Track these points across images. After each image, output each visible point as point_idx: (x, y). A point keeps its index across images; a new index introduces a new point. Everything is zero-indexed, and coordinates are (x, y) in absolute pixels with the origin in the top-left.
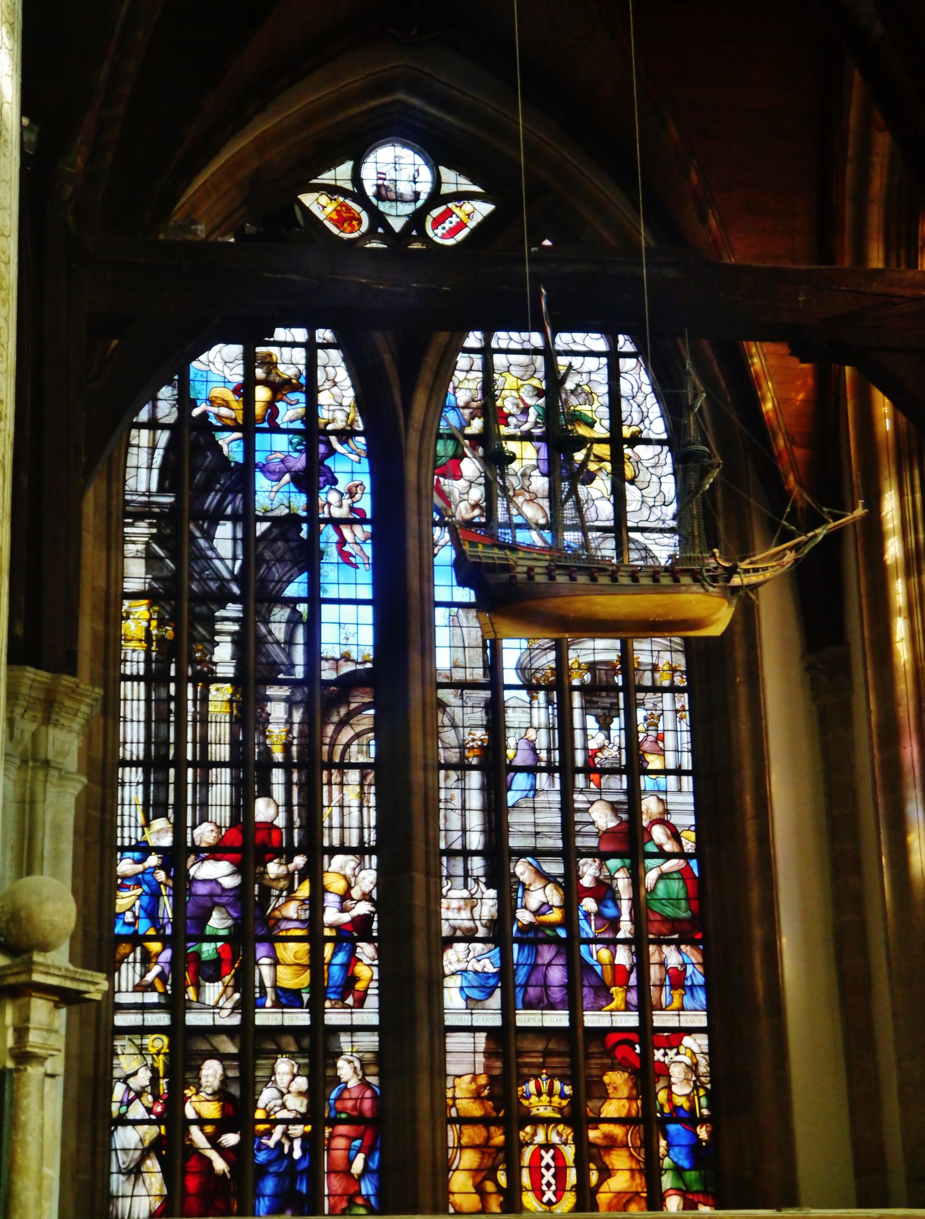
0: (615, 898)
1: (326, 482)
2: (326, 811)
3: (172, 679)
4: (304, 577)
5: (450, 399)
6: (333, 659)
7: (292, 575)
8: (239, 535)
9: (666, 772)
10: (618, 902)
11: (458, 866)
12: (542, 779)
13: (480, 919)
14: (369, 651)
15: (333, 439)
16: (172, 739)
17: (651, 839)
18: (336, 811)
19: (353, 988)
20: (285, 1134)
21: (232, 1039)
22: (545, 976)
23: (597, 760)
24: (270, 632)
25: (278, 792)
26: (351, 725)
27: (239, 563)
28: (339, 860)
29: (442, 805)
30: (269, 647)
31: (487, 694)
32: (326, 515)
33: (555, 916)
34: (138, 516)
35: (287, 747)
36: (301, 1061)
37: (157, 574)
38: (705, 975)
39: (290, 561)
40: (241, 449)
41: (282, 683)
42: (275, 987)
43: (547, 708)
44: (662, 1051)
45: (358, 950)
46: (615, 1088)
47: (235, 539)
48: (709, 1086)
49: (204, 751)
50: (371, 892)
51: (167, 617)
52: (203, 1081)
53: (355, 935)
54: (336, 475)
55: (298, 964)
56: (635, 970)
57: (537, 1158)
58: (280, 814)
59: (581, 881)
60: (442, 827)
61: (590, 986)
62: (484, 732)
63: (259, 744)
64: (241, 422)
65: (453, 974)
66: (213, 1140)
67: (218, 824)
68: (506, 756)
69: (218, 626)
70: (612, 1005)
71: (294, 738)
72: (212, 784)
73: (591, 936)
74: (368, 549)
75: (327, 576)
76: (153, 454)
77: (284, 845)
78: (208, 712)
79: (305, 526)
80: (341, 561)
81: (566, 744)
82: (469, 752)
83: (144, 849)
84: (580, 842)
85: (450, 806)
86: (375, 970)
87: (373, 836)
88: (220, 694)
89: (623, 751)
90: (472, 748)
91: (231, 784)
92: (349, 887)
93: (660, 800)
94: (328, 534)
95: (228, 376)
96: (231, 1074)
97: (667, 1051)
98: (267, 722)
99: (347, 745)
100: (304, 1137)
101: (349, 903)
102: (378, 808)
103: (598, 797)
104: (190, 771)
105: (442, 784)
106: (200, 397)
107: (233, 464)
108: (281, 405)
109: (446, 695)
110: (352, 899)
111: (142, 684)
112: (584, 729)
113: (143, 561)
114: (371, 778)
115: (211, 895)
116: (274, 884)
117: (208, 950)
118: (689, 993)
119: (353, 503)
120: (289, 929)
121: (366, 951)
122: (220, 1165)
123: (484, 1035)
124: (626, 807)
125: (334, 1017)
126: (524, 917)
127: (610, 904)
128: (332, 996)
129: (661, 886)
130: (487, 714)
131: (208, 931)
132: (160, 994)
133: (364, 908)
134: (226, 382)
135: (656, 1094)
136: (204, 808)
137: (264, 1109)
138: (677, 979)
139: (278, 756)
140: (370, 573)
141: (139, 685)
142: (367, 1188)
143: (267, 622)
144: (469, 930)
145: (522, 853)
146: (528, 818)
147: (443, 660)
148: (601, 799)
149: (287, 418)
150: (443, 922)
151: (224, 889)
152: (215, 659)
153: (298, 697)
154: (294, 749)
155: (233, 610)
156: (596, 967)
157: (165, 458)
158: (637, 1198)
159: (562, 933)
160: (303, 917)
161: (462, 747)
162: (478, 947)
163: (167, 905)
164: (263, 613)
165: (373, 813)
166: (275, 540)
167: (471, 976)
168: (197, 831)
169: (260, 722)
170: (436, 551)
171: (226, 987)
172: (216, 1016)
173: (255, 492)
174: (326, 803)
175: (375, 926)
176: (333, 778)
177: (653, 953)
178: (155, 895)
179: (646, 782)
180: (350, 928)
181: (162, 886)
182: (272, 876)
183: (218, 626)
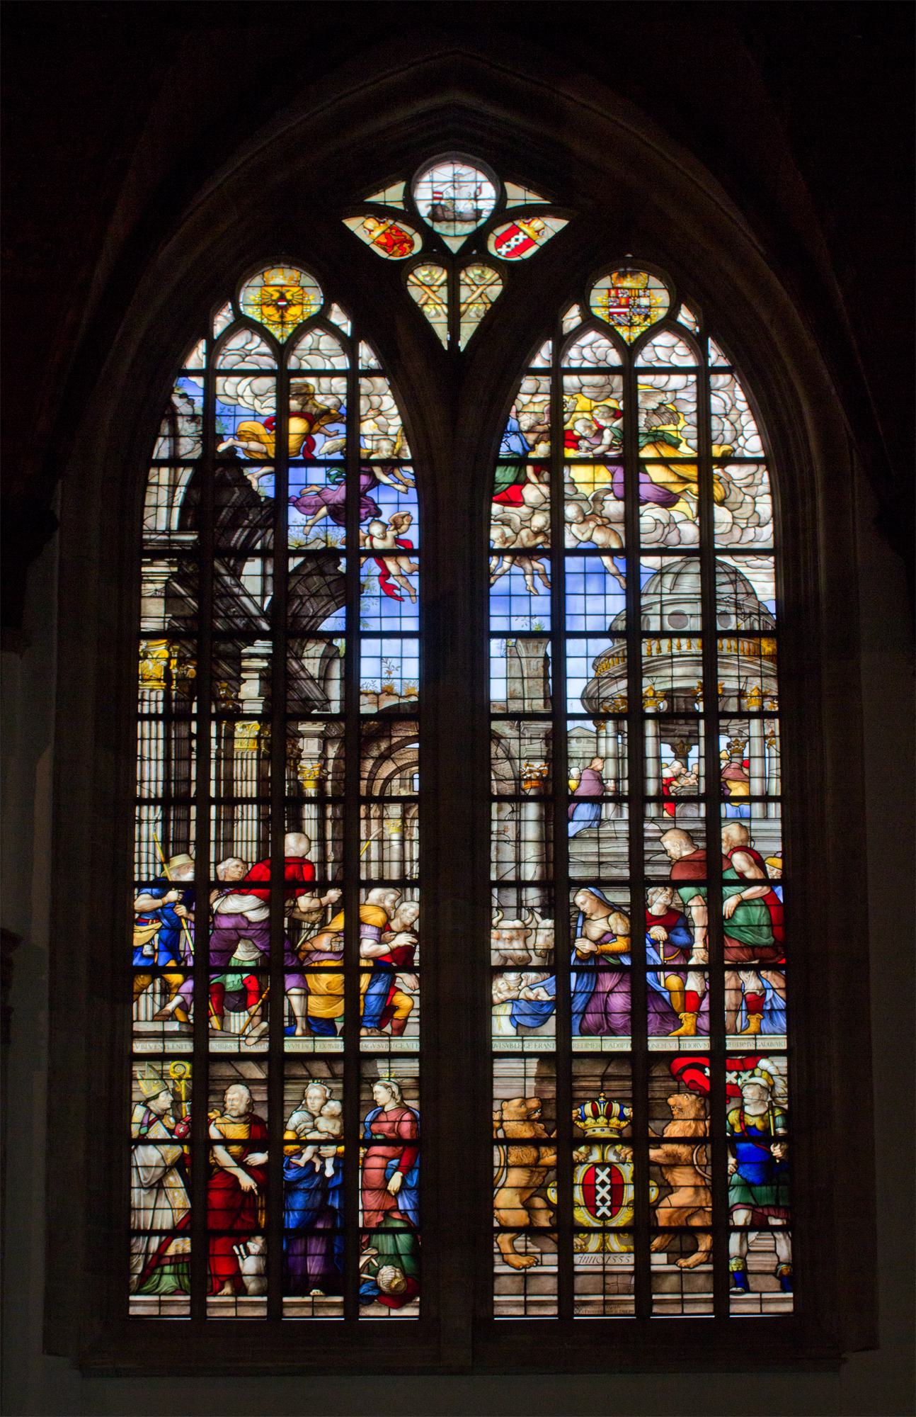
0: (688, 926)
1: (369, 514)
2: (364, 846)
3: (194, 717)
4: (342, 611)
5: (512, 424)
6: (374, 693)
7: (328, 610)
8: (270, 570)
9: (750, 799)
10: (691, 930)
11: (511, 897)
12: (609, 810)
13: (534, 949)
14: (415, 686)
15: (377, 471)
16: (194, 777)
17: (732, 867)
18: (374, 845)
19: (392, 1017)
20: (317, 1154)
21: (260, 1066)
22: (606, 1003)
23: (671, 789)
24: (303, 668)
25: (311, 827)
26: (392, 759)
27: (268, 599)
28: (376, 893)
29: (494, 837)
30: (302, 683)
31: (548, 725)
32: (368, 547)
33: (620, 944)
34: (157, 555)
35: (320, 783)
36: (333, 1086)
37: (178, 613)
38: (787, 1001)
39: (327, 596)
40: (273, 483)
41: (315, 719)
42: (306, 1017)
43: (616, 737)
44: (735, 1074)
45: (398, 980)
46: (681, 1110)
47: (264, 575)
48: (786, 1107)
49: (229, 788)
50: (412, 923)
51: (188, 655)
52: (228, 1104)
53: (394, 964)
54: (380, 506)
55: (331, 995)
56: (707, 996)
57: (591, 1176)
58: (313, 849)
59: (650, 910)
60: (493, 859)
61: (657, 1012)
62: (543, 763)
63: (289, 780)
64: (273, 456)
65: (503, 1002)
66: (241, 1163)
67: (244, 859)
68: (568, 786)
69: (245, 664)
70: (681, 1031)
71: (329, 773)
72: (238, 820)
73: (659, 963)
74: (415, 582)
75: (368, 610)
76: (174, 492)
77: (317, 879)
78: (233, 749)
79: (343, 561)
80: (383, 594)
82: (526, 783)
83: (162, 885)
84: (649, 871)
85: (503, 837)
86: (417, 999)
87: (416, 869)
88: (246, 733)
89: (703, 780)
90: (530, 779)
91: (258, 820)
92: (389, 919)
93: (742, 827)
94: (370, 567)
95: (258, 410)
96: (257, 1098)
97: (741, 1073)
98: (299, 758)
99: (389, 779)
100: (336, 1157)
101: (388, 935)
102: (420, 841)
103: (672, 825)
104: (213, 808)
105: (494, 816)
106: (227, 432)
107: (263, 499)
108: (318, 438)
110: (391, 931)
111: (161, 724)
112: (658, 758)
113: (162, 601)
114: (414, 811)
115: (236, 929)
116: (305, 917)
117: (232, 981)
118: (767, 1017)
119: (399, 534)
120: (322, 961)
121: (407, 981)
122: (246, 1182)
123: (536, 1060)
124: (704, 835)
125: (369, 1044)
126: (584, 946)
127: (682, 931)
128: (368, 1025)
129: (741, 913)
130: (547, 745)
131: (233, 963)
132: (181, 1023)
133: (403, 940)
134: (256, 415)
135: (727, 1116)
136: (229, 845)
137: (294, 1131)
138: (755, 1005)
139: (311, 790)
140: (417, 604)
141: (157, 724)
142: (404, 1203)
143: (299, 658)
144: (522, 959)
145: (582, 884)
146: (593, 848)
147: (498, 691)
148: (675, 828)
149: (324, 450)
150: (492, 952)
151: (250, 923)
152: (241, 696)
153: (334, 732)
154: (329, 784)
155: (262, 646)
156: (663, 994)
157: (187, 495)
158: (701, 1212)
159: (627, 961)
160: (337, 949)
161: (518, 779)
162: (533, 975)
163: (189, 938)
164: (295, 650)
165: (416, 846)
166: (309, 575)
167: (523, 1004)
168: (221, 867)
169: (291, 758)
170: (492, 580)
171: (252, 1017)
172: (242, 1044)
173: (287, 527)
174: (363, 836)
175: (417, 956)
176: (372, 812)
177: (729, 979)
178: (174, 929)
179: (727, 810)
180: (386, 959)
181: (183, 920)
182: (303, 910)
183: (245, 664)
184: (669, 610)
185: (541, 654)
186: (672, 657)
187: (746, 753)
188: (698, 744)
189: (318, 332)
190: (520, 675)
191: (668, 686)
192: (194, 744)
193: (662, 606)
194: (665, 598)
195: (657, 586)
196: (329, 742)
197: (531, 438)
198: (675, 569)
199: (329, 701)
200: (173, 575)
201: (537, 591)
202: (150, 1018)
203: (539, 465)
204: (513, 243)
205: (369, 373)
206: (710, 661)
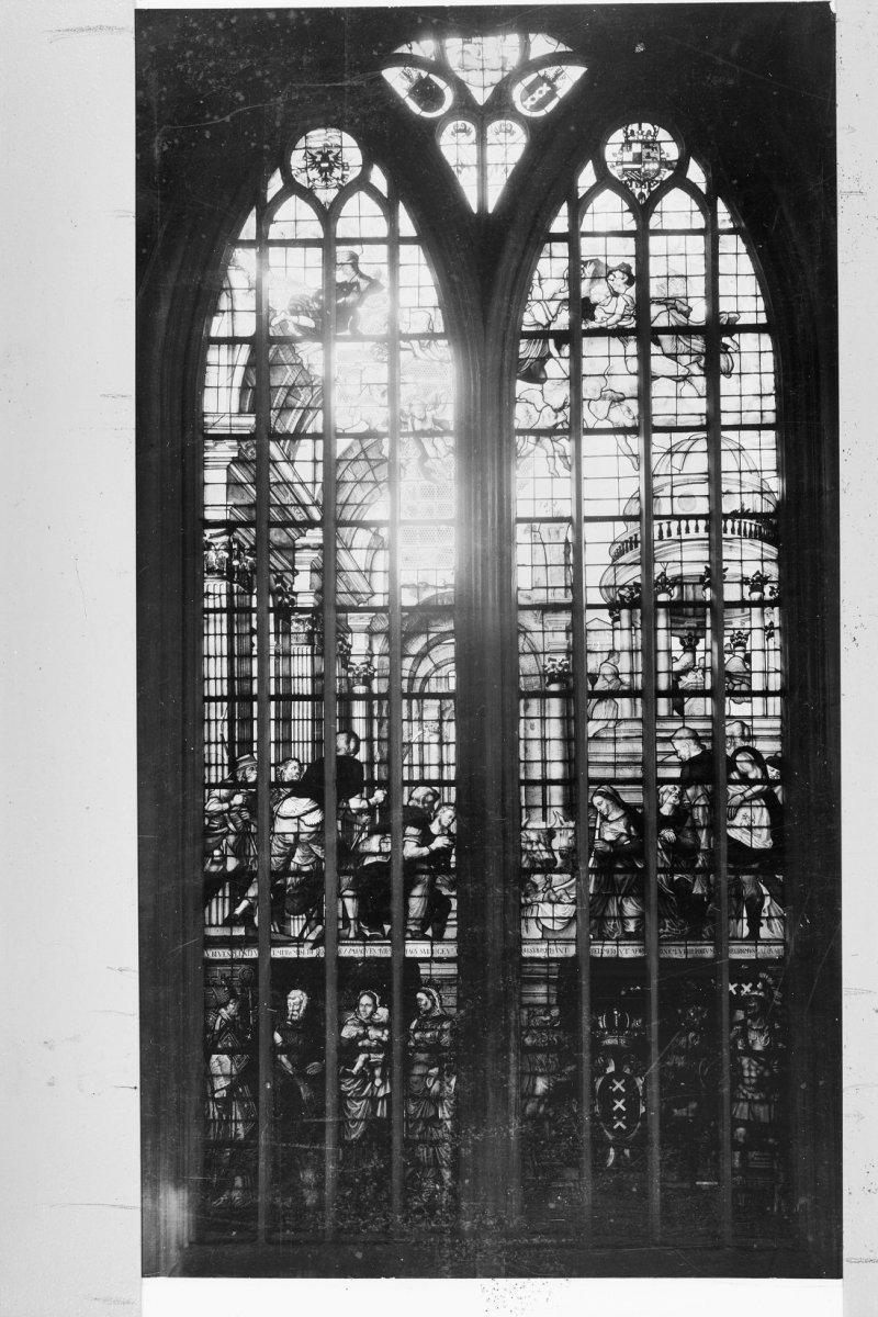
62: (564, 657)
81: (651, 671)
91: (313, 720)
103: (681, 725)
105: (522, 714)
109: (528, 620)
112: (669, 651)
130: (567, 638)
133: (440, 842)
148: (684, 727)
155: (315, 536)
166: (356, 460)
175: (453, 859)
187: (748, 648)
188: (704, 637)
189: (362, 194)
192: (255, 639)
196: (374, 637)
197: (554, 306)
198: (684, 449)
200: (234, 461)
203: (561, 338)
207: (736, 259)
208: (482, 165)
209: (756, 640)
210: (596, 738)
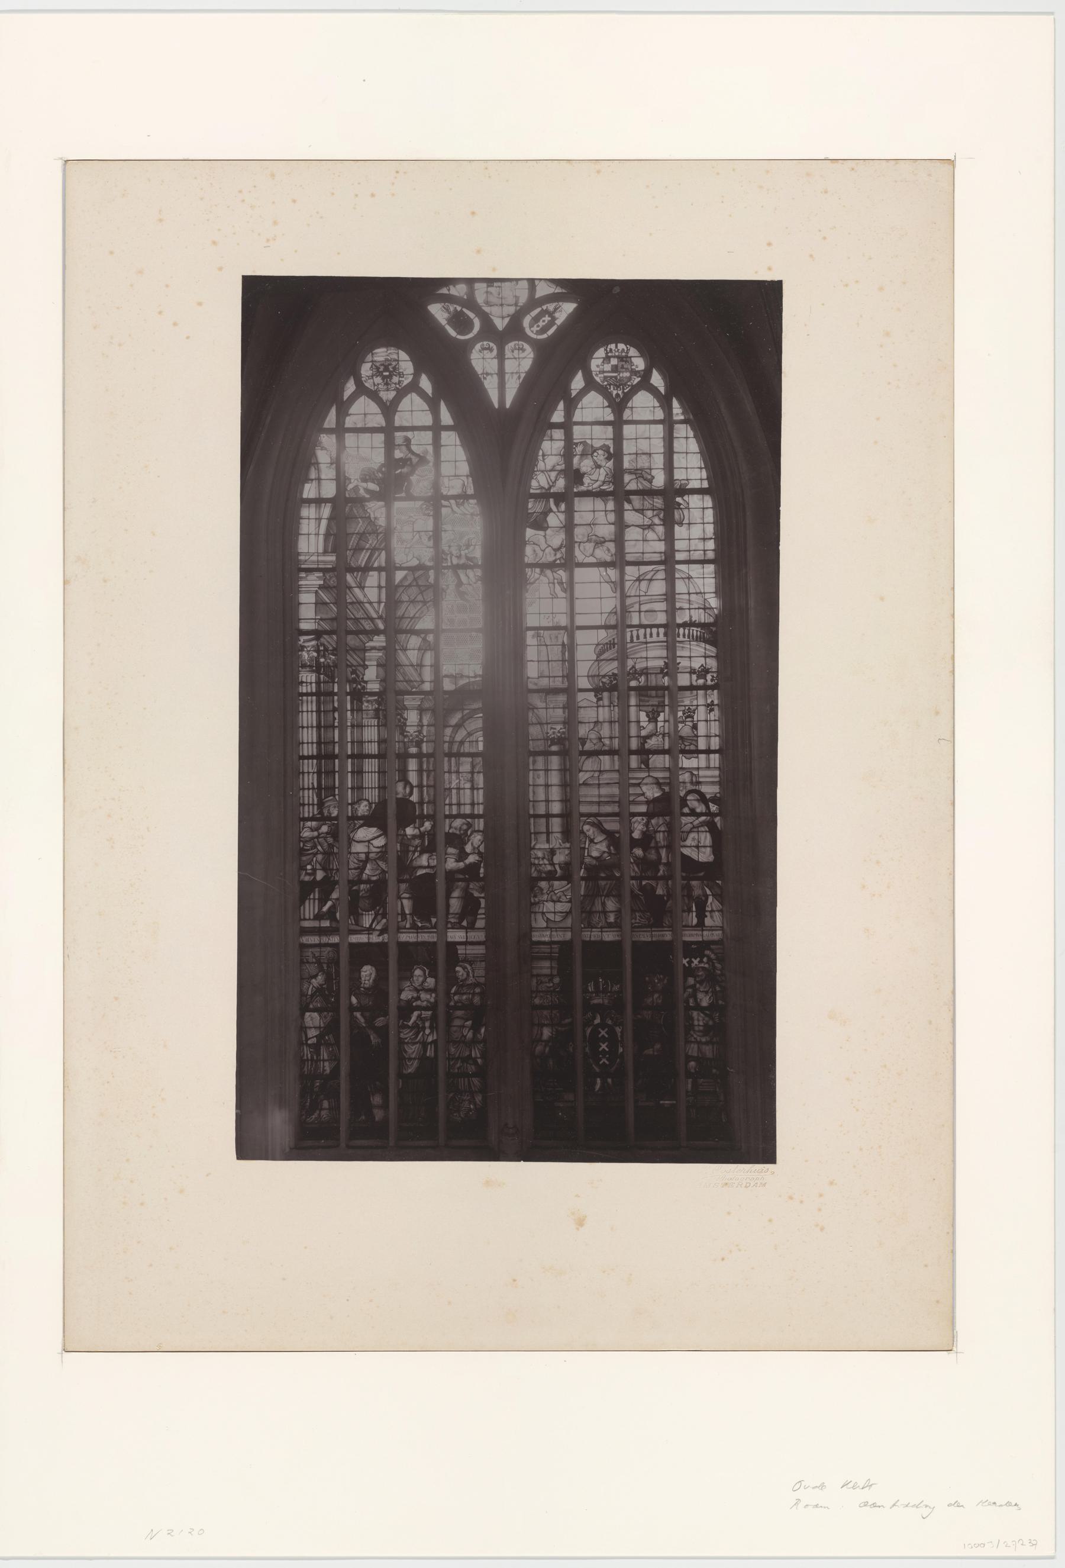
30: (406, 668)
47: (380, 587)
62: (562, 727)
91: (379, 772)
103: (647, 774)
109: (536, 700)
112: (638, 722)
130: (564, 713)
133: (472, 859)
144: (550, 872)
148: (649, 776)
155: (379, 641)
166: (410, 586)
175: (482, 870)
184: (644, 608)
185: (560, 642)
186: (646, 643)
187: (695, 719)
188: (664, 711)
189: (414, 395)
190: (546, 659)
191: (644, 665)
192: (336, 715)
193: (640, 605)
194: (642, 598)
195: (636, 590)
197: (553, 475)
198: (648, 577)
199: (423, 682)
200: (321, 587)
201: (557, 596)
202: (312, 917)
203: (559, 498)
204: (541, 324)
205: (447, 428)
206: (671, 646)
207: (687, 442)
208: (501, 373)
209: (701, 714)
210: (585, 784)
